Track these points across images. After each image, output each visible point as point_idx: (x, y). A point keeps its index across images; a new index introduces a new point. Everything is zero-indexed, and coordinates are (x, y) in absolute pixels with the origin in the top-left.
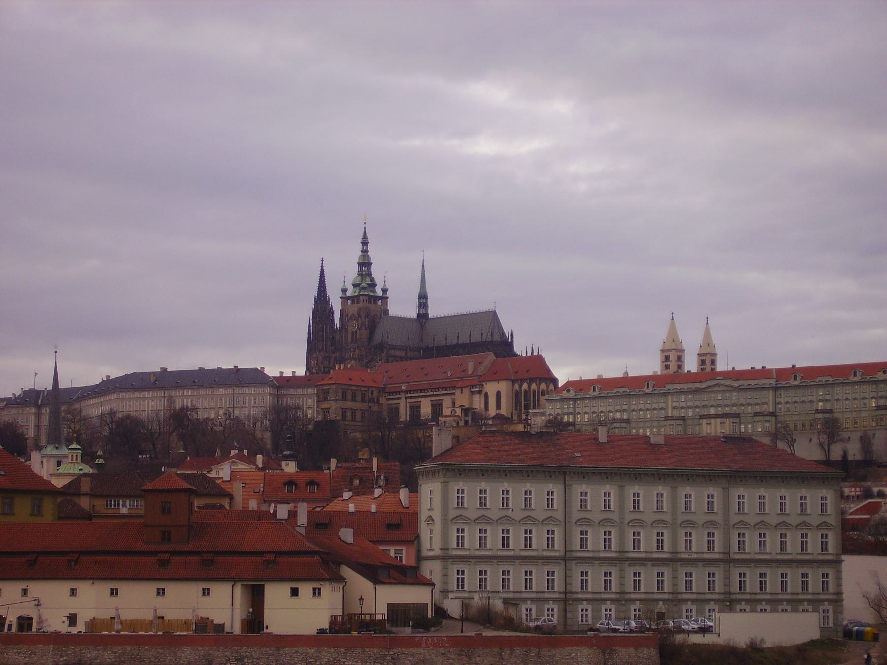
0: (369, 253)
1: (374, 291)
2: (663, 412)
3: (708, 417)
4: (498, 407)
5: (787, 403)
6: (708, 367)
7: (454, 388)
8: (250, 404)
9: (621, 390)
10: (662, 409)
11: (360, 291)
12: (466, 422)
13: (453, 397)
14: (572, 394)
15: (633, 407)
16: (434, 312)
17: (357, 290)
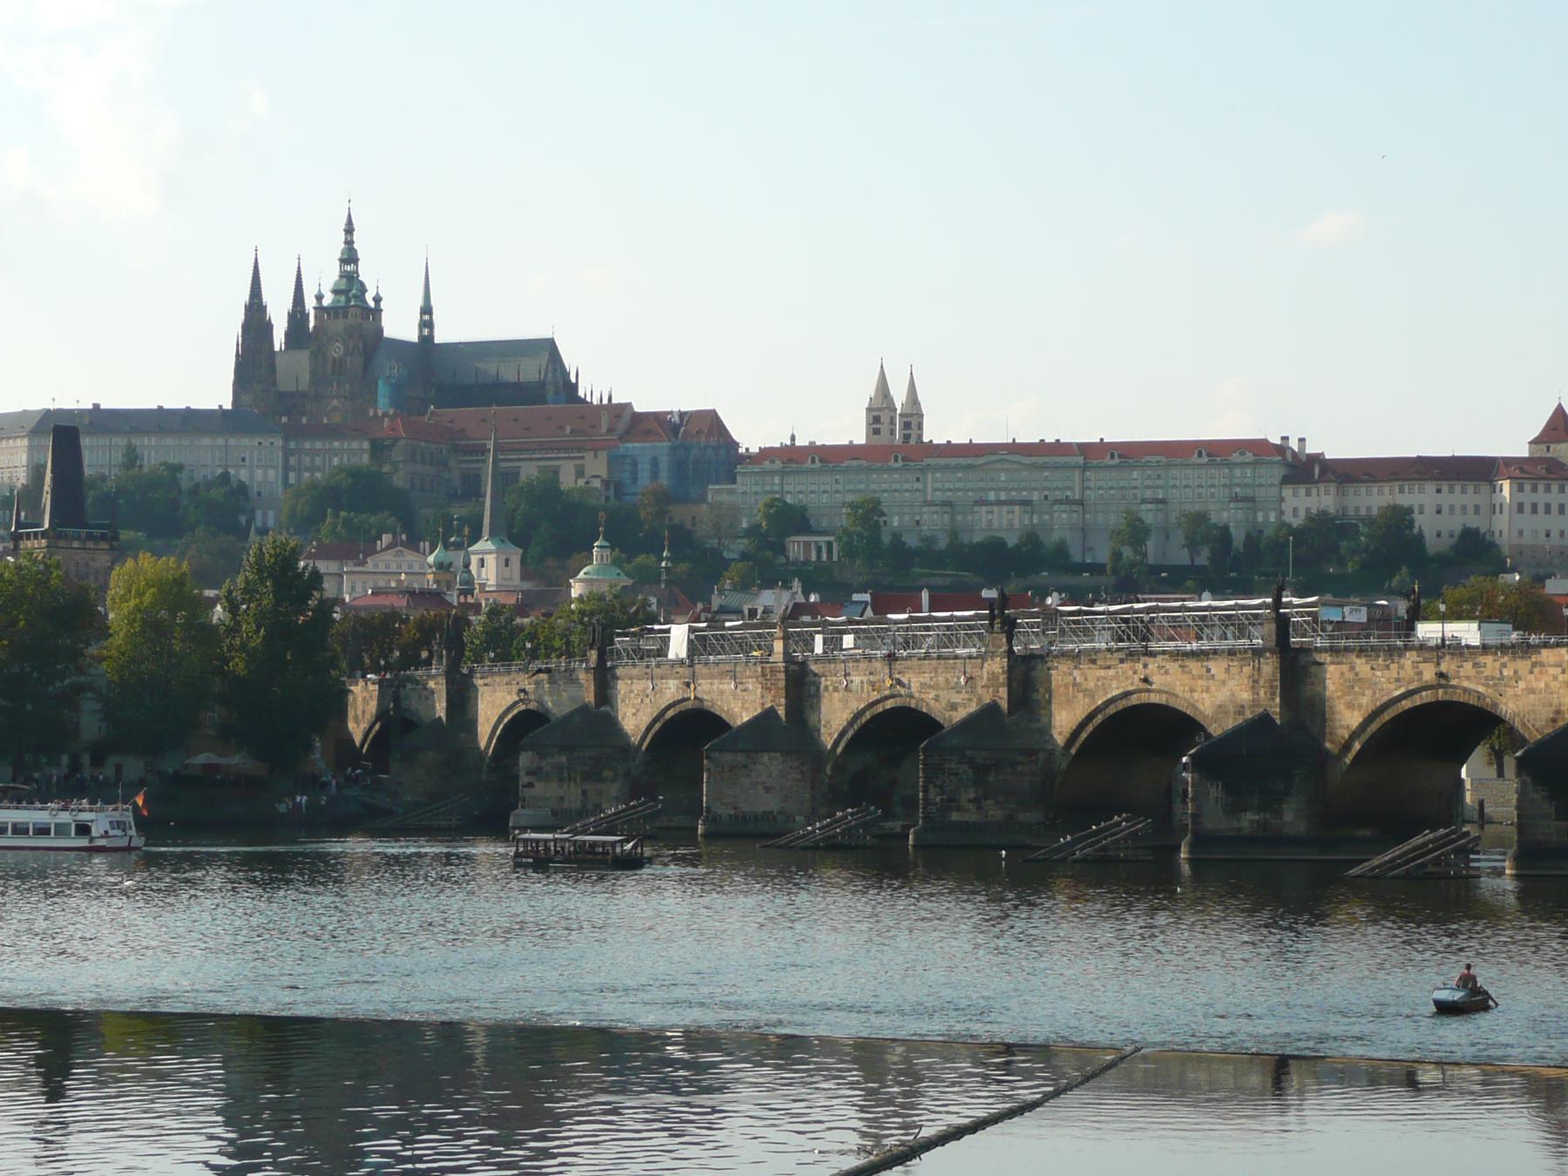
0: (355, 246)
1: (366, 302)
2: (918, 494)
3: (991, 504)
4: (655, 475)
5: (1100, 488)
6: (913, 432)
7: (579, 450)
8: (252, 461)
9: (855, 463)
10: (920, 491)
11: (348, 300)
12: (607, 498)
13: (578, 462)
14: (778, 465)
15: (873, 487)
16: (440, 337)
17: (343, 299)
